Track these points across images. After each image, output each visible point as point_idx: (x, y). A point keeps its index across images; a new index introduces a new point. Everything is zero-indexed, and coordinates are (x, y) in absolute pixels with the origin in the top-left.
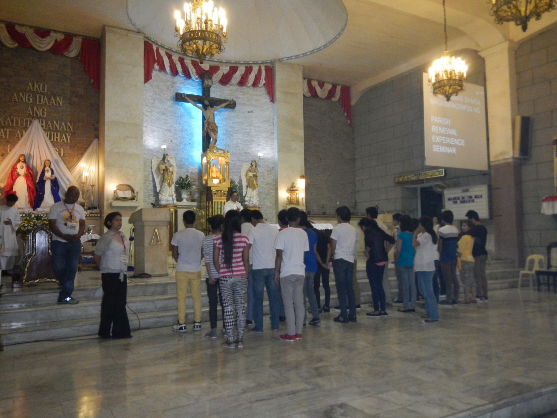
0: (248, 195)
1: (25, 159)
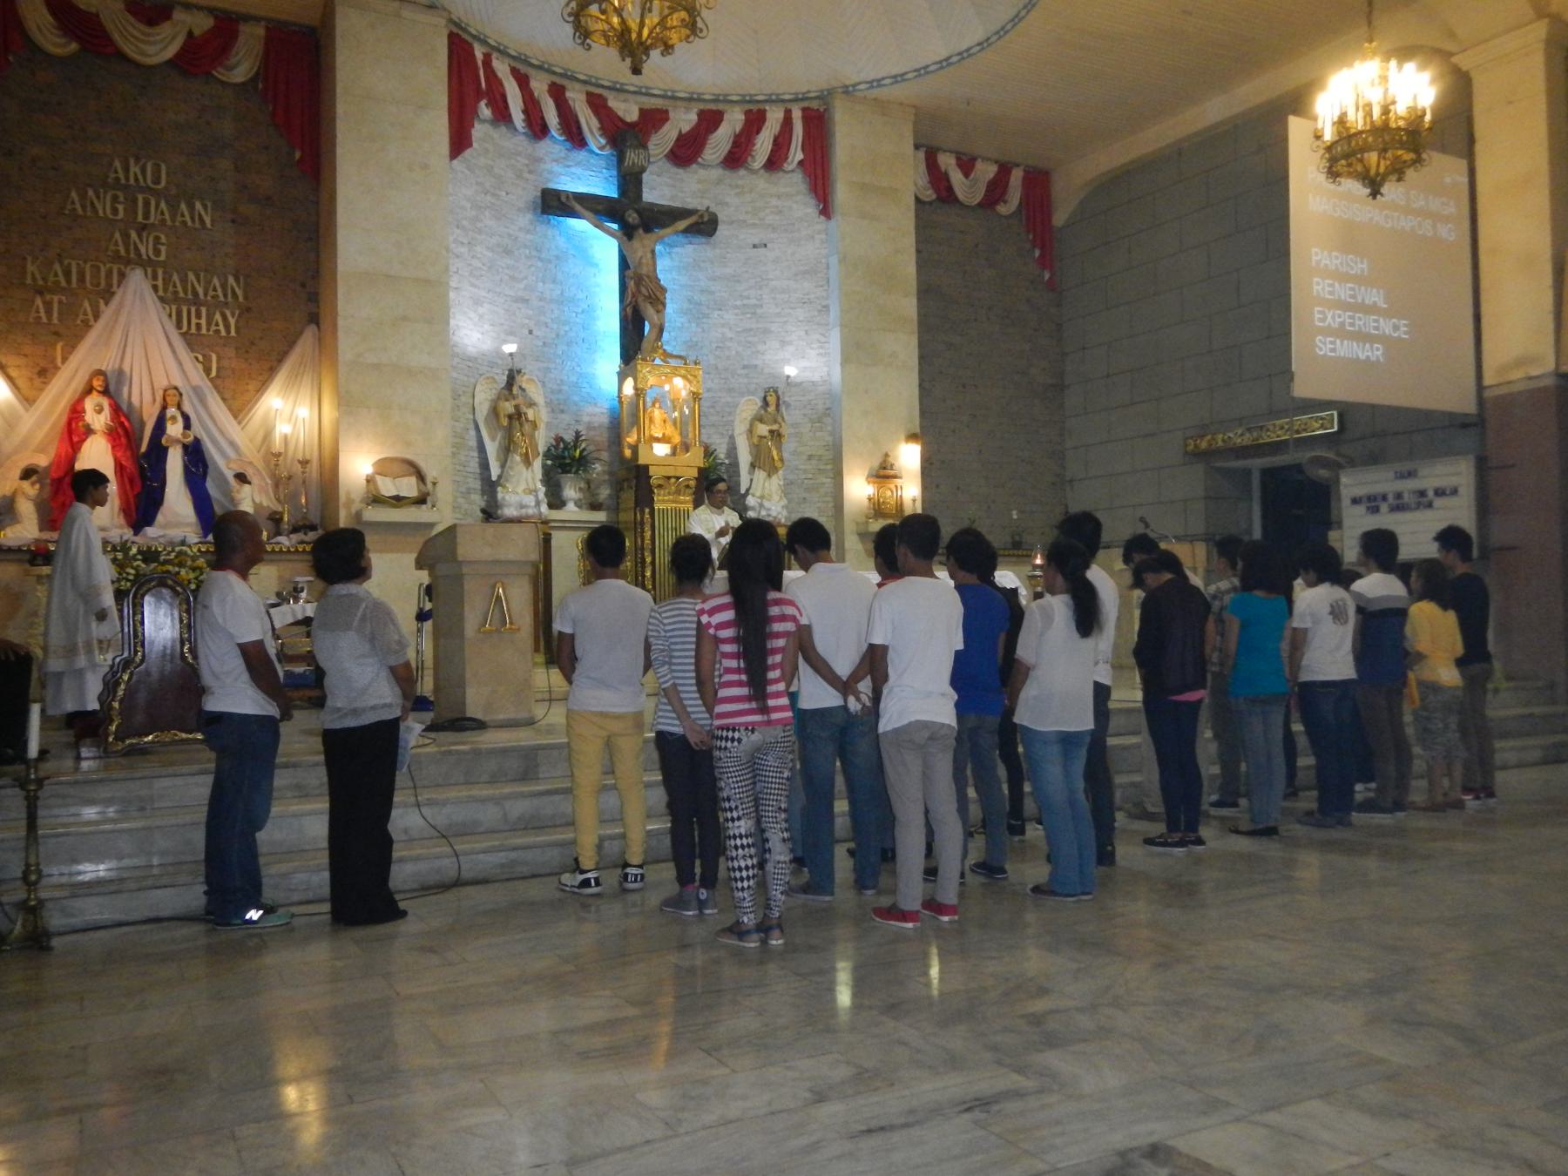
0: (757, 490)
1: (108, 386)
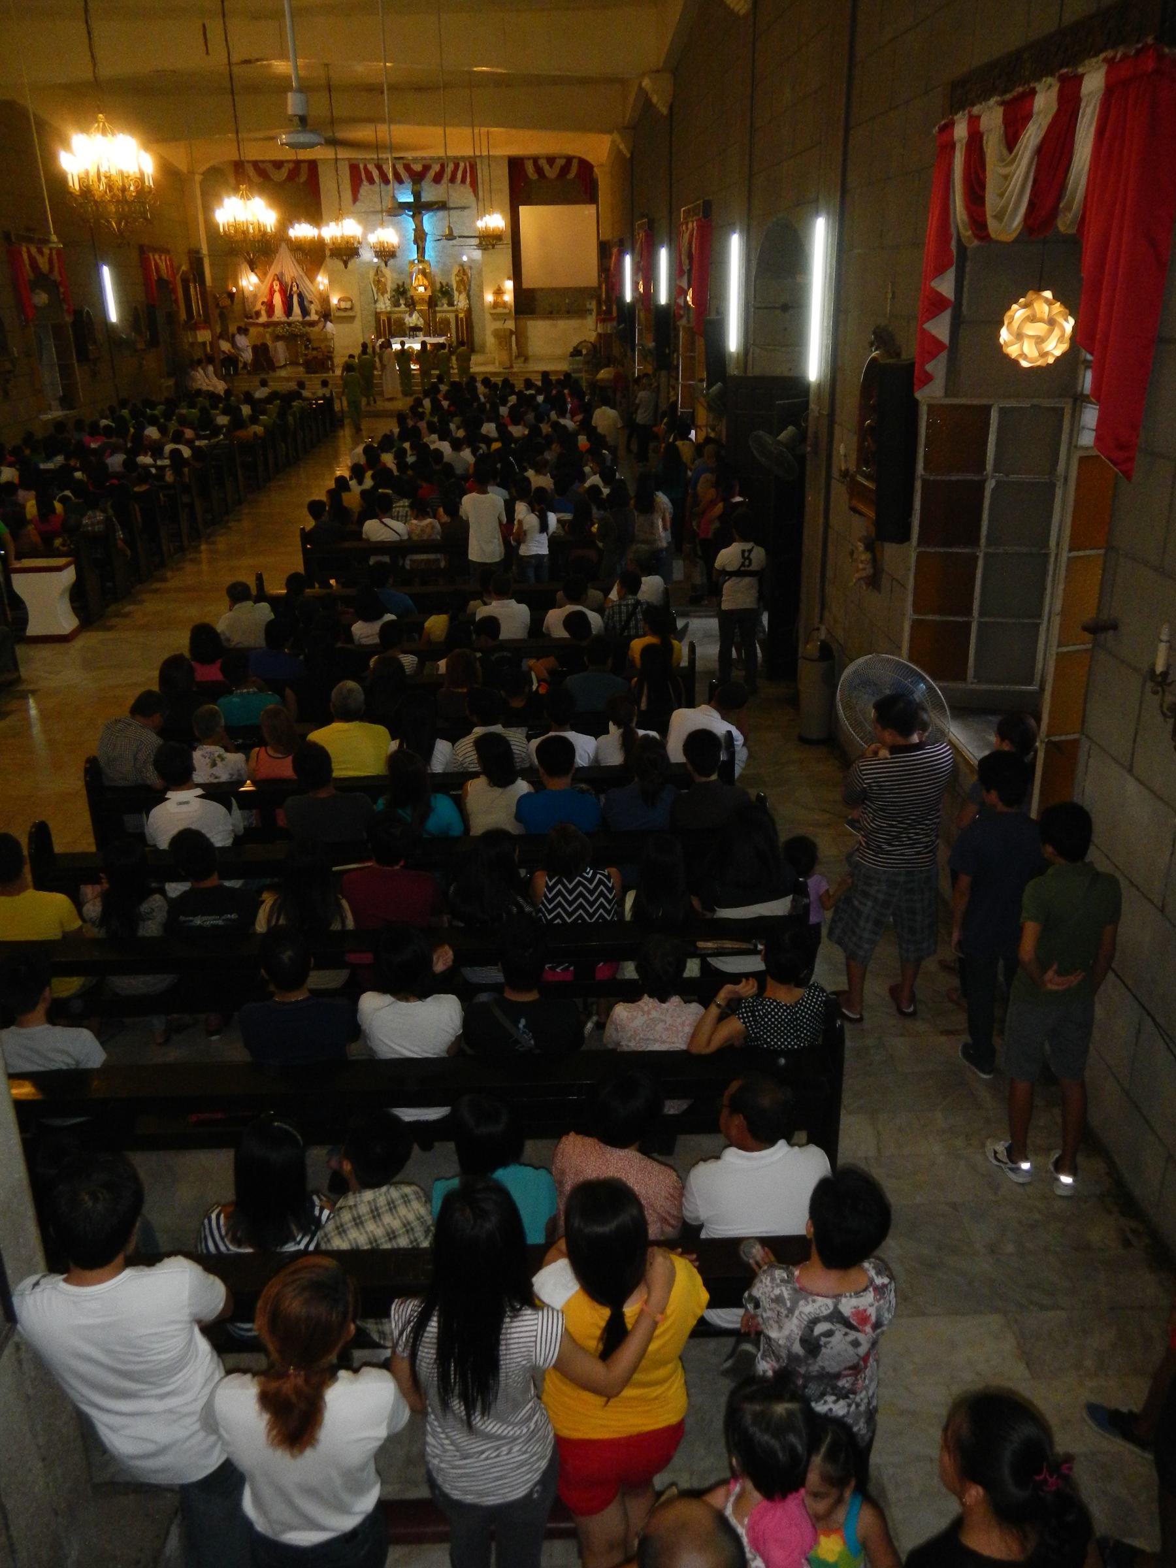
1: (279, 278)
